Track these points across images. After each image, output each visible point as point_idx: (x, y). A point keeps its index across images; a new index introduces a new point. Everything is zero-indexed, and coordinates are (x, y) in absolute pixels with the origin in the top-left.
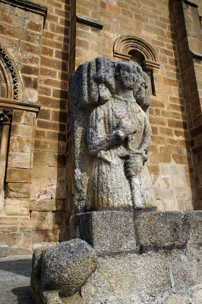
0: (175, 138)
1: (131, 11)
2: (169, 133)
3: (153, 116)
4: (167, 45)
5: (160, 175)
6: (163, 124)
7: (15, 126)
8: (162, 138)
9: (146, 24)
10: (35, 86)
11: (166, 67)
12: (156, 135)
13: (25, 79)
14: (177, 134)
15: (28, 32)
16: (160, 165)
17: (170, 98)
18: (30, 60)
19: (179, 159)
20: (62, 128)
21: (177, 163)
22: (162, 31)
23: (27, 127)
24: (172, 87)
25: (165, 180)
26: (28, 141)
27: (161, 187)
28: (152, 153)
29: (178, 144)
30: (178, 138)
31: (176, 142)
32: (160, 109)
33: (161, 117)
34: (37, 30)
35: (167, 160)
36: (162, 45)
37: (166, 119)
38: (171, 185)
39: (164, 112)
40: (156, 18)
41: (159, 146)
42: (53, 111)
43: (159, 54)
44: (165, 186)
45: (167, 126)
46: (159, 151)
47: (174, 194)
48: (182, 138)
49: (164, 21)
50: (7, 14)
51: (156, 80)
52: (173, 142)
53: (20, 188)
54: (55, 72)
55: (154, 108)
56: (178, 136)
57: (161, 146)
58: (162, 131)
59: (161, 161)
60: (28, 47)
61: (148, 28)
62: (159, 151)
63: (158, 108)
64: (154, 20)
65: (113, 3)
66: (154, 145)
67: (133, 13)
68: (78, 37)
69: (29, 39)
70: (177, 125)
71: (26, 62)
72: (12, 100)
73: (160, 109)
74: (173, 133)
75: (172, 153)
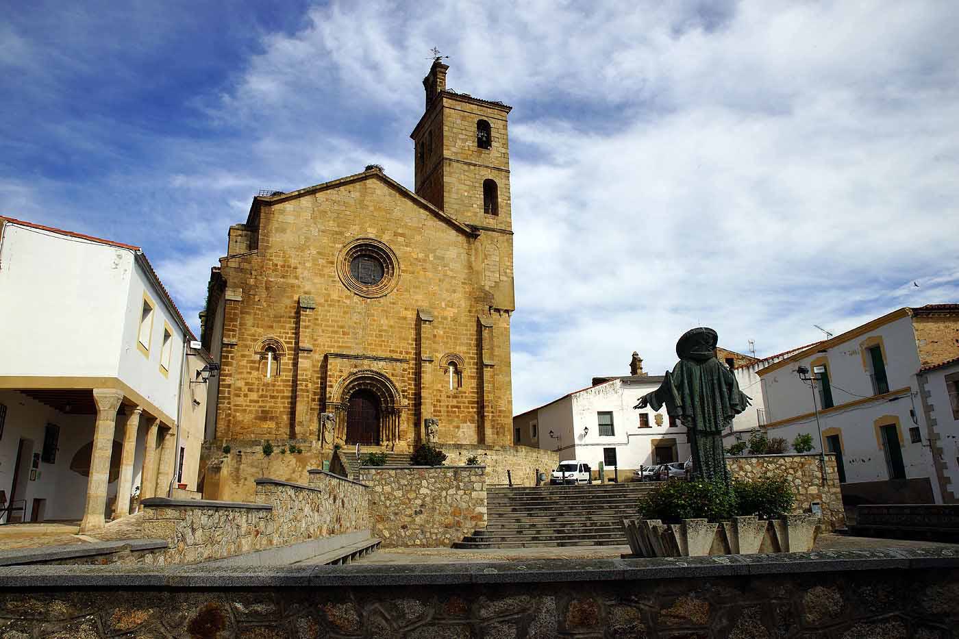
0: (471, 410)
2: (468, 407)
3: (459, 400)
11: (471, 368)
13: (403, 395)
14: (472, 408)
16: (461, 425)
19: (472, 421)
20: (415, 410)
36: (469, 353)
40: (467, 335)
41: (461, 415)
43: (467, 360)
48: (475, 410)
52: (469, 412)
61: (462, 344)
68: (422, 369)
70: (473, 403)
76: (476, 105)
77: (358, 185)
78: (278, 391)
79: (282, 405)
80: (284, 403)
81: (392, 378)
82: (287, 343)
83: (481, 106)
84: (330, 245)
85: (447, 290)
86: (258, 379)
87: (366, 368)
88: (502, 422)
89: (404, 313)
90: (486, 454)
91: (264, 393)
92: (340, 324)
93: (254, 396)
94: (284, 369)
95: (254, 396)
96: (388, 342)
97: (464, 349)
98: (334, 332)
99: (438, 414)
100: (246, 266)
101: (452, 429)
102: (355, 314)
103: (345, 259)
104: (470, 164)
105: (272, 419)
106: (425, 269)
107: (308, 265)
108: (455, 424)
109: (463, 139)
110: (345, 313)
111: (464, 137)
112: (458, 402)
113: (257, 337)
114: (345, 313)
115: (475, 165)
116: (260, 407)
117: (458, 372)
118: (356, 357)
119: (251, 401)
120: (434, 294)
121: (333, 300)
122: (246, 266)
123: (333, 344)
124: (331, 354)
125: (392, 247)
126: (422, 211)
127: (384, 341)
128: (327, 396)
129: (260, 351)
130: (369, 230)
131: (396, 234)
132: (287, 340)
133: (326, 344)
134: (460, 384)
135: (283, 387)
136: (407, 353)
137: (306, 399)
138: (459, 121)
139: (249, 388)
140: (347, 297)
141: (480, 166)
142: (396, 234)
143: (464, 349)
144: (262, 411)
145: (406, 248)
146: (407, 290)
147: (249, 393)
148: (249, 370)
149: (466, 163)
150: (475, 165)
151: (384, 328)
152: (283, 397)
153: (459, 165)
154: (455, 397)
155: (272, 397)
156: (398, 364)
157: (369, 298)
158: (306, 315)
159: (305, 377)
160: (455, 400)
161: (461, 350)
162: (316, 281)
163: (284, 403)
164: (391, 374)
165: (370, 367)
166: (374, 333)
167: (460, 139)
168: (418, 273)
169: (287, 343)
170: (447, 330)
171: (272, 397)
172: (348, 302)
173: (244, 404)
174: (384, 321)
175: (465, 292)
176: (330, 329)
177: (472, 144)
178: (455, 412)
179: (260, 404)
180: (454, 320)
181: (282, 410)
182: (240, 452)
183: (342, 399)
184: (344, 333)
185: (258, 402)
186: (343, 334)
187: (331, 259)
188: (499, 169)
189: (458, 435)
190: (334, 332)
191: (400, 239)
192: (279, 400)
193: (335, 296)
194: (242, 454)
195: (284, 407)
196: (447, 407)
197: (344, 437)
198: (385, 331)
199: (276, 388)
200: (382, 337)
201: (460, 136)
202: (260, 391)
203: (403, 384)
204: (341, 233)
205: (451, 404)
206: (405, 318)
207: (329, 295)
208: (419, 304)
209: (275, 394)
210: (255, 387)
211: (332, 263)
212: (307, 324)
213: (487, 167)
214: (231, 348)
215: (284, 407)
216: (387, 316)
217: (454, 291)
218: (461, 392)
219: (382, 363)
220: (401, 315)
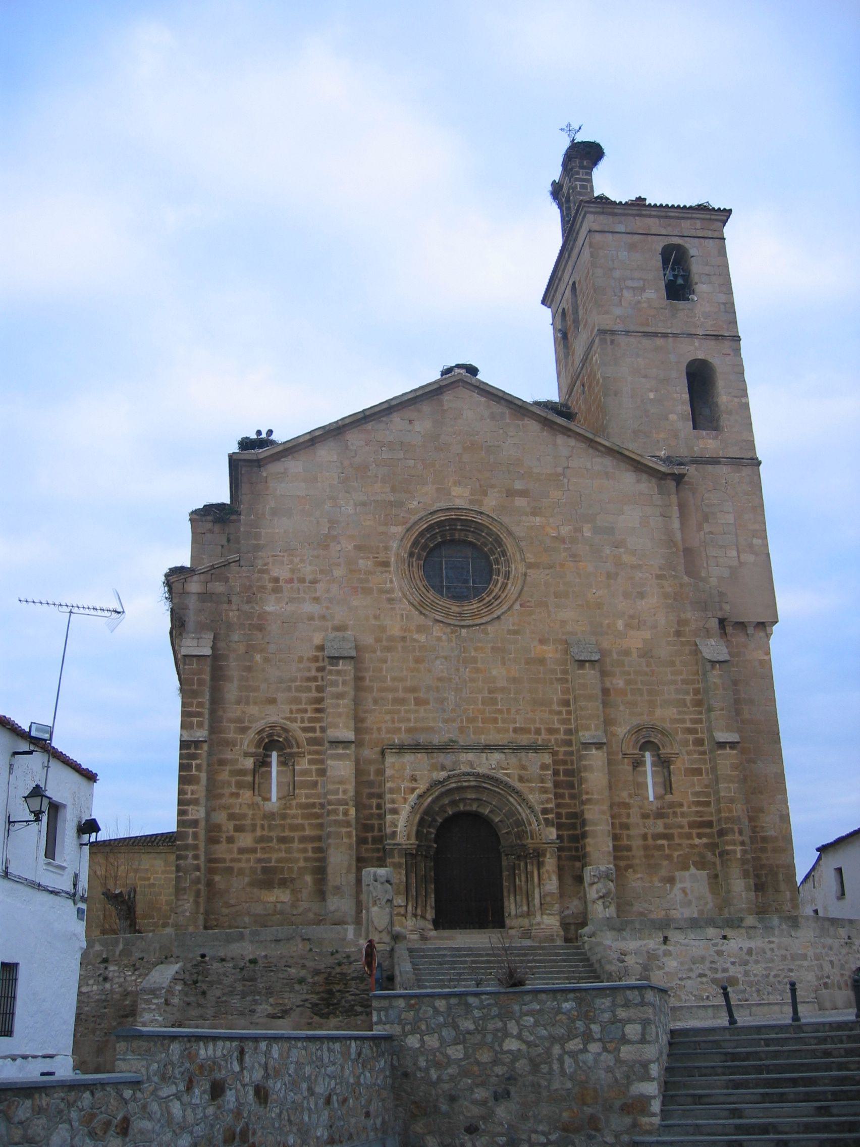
0: (697, 841)
1: (641, 687)
2: (689, 836)
4: (691, 719)
7: (543, 862)
8: (680, 845)
10: (553, 826)
11: (688, 753)
12: (673, 842)
13: (545, 819)
15: (541, 775)
17: (692, 793)
21: (698, 869)
22: (684, 700)
23: (551, 861)
24: (695, 778)
25: (684, 890)
26: (553, 871)
30: (700, 841)
31: (696, 845)
32: (678, 810)
33: (680, 819)
34: (548, 770)
35: (686, 868)
36: (683, 721)
37: (684, 821)
39: (683, 815)
40: (674, 682)
41: (676, 854)
42: (567, 835)
45: (687, 830)
46: (675, 860)
49: (687, 684)
51: (674, 774)
52: (693, 846)
54: (564, 794)
56: (700, 838)
58: (681, 836)
60: (543, 790)
62: (675, 860)
63: (675, 810)
64: (672, 687)
65: (618, 684)
67: (645, 687)
69: (542, 781)
71: (543, 804)
72: (538, 841)
73: (678, 810)
74: (694, 835)
76: (654, 216)
77: (426, 408)
78: (293, 828)
79: (302, 856)
80: (305, 850)
81: (518, 785)
82: (305, 730)
83: (666, 217)
84: (382, 529)
85: (626, 595)
86: (253, 806)
87: (465, 769)
89: (538, 649)
90: (725, 937)
91: (265, 833)
92: (409, 684)
93: (246, 840)
94: (302, 782)
95: (246, 840)
96: (509, 711)
97: (671, 712)
98: (396, 701)
100: (218, 587)
102: (438, 662)
103: (411, 555)
104: (655, 334)
105: (283, 883)
107: (338, 572)
108: (663, 873)
109: (633, 289)
110: (418, 661)
111: (636, 284)
112: (666, 826)
113: (246, 724)
114: (418, 661)
115: (665, 335)
116: (259, 861)
117: (664, 763)
118: (445, 748)
119: (242, 851)
120: (599, 606)
121: (391, 639)
122: (218, 587)
123: (396, 725)
124: (392, 746)
125: (505, 519)
127: (500, 711)
128: (389, 830)
129: (254, 750)
130: (456, 491)
131: (511, 493)
132: (306, 724)
133: (384, 726)
134: (668, 786)
135: (302, 818)
136: (551, 731)
137: (345, 840)
138: (623, 255)
139: (235, 826)
140: (420, 629)
141: (675, 335)
142: (511, 493)
143: (671, 712)
144: (265, 870)
145: (532, 518)
147: (237, 834)
148: (234, 790)
149: (646, 334)
150: (665, 335)
151: (501, 683)
152: (303, 839)
153: (632, 340)
154: (660, 815)
155: (283, 840)
156: (532, 755)
157: (463, 627)
158: (338, 673)
159: (341, 796)
160: (660, 822)
161: (665, 715)
162: (355, 603)
163: (305, 850)
164: (516, 777)
165: (472, 766)
166: (480, 697)
167: (628, 288)
168: (562, 566)
169: (305, 730)
170: (632, 676)
171: (283, 840)
172: (422, 638)
173: (228, 856)
174: (498, 672)
175: (666, 596)
176: (390, 696)
177: (655, 294)
179: (259, 855)
180: (646, 654)
181: (302, 864)
182: (203, 956)
183: (418, 834)
184: (419, 702)
185: (254, 851)
186: (416, 704)
187: (382, 557)
188: (717, 337)
190: (396, 701)
191: (520, 502)
192: (296, 845)
193: (395, 630)
194: (207, 958)
195: (306, 859)
196: (645, 837)
197: (430, 914)
198: (503, 689)
199: (289, 821)
200: (496, 704)
201: (629, 283)
202: (258, 829)
203: (545, 796)
204: (400, 504)
206: (542, 661)
207: (383, 629)
208: (569, 628)
209: (287, 833)
210: (248, 822)
211: (386, 564)
212: (340, 689)
213: (691, 335)
214: (196, 748)
215: (306, 859)
216: (503, 658)
217: (642, 595)
218: (672, 805)
219: (496, 757)
220: (533, 656)
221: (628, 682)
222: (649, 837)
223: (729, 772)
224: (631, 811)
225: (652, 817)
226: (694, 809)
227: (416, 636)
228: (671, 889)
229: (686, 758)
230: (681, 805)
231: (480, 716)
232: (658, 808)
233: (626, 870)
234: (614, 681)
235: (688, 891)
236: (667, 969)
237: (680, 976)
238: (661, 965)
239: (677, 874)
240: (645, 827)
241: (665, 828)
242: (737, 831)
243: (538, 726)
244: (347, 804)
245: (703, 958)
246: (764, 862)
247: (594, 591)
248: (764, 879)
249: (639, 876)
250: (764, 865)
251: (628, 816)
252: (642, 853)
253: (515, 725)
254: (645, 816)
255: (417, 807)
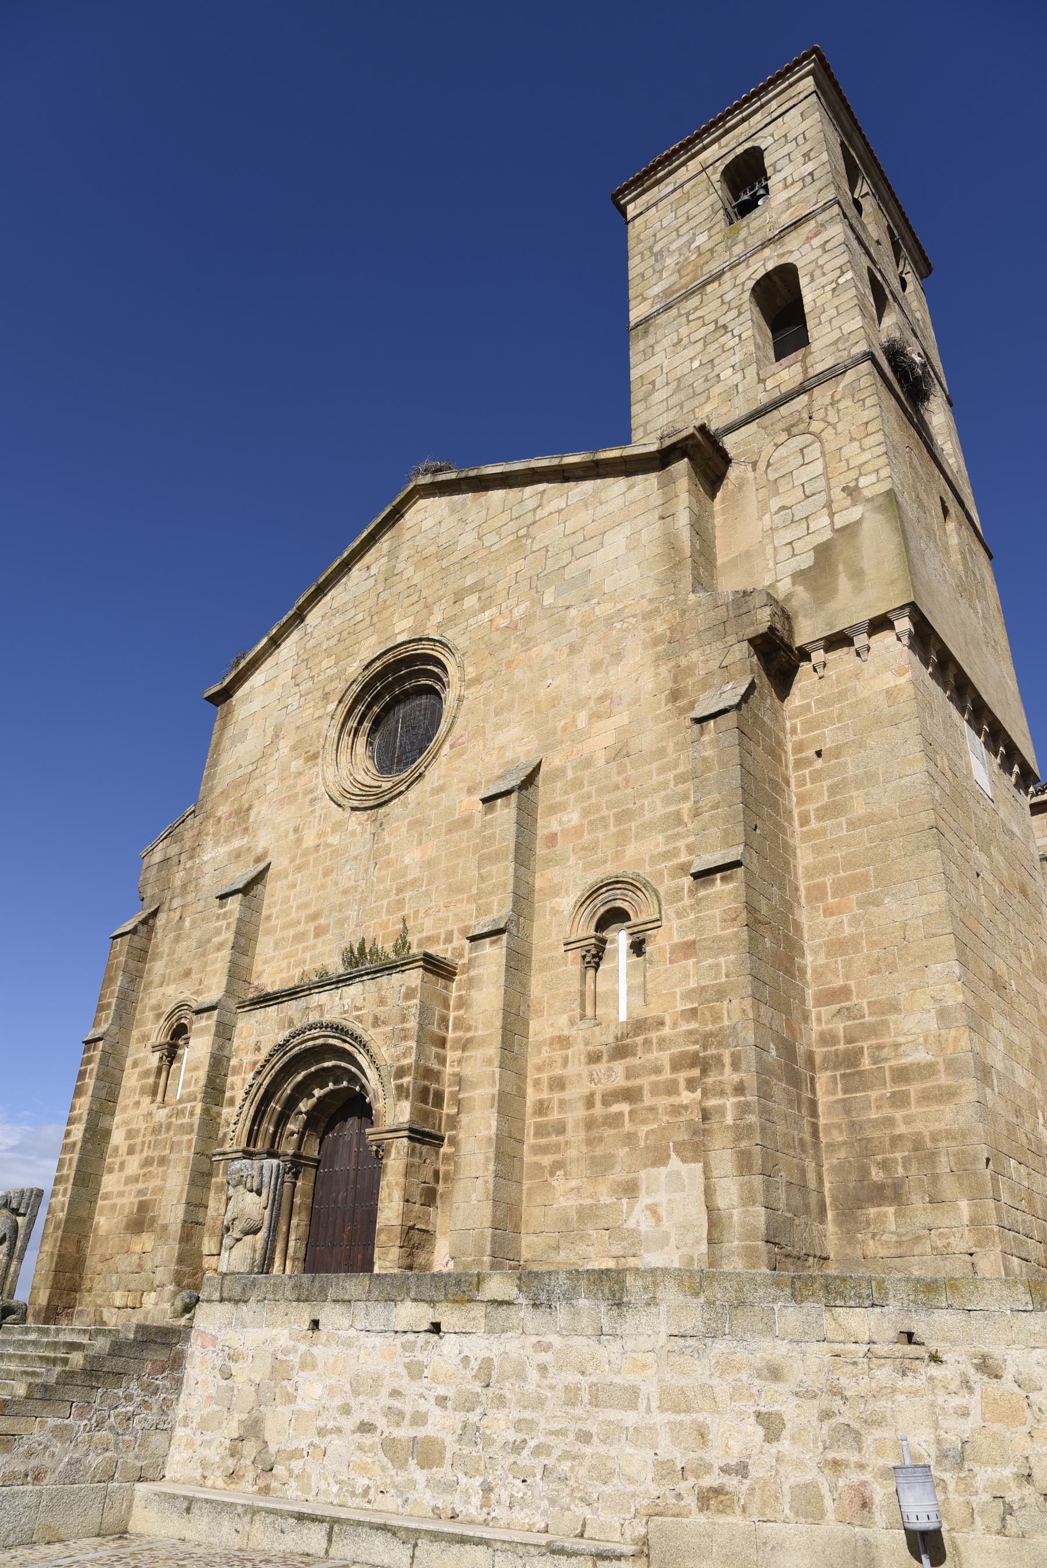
2: (671, 1088)
5: (641, 1199)
6: (658, 1070)
8: (652, 1109)
9: (640, 821)
12: (639, 1105)
18: (404, 1054)
21: (684, 1160)
25: (653, 1210)
26: (397, 1184)
27: (643, 1228)
28: (627, 1149)
29: (691, 1113)
31: (686, 1107)
32: (653, 1035)
33: (656, 1054)
35: (659, 1158)
38: (665, 1220)
44: (652, 1222)
45: (667, 1075)
46: (642, 1143)
47: (673, 1242)
49: (685, 781)
50: (383, 993)
52: (676, 1110)
53: (387, 1254)
55: (639, 1040)
57: (647, 1128)
59: (645, 1166)
60: (402, 1035)
62: (642, 1143)
64: (657, 798)
66: (632, 1129)
74: (682, 1085)
75: (675, 1139)
88: (918, 1126)
90: (436, 1328)
99: (554, 1139)
101: (605, 1199)
106: (528, 644)
108: (619, 1174)
110: (327, 873)
112: (630, 1073)
126: (529, 490)
140: (338, 827)
146: (479, 732)
178: (615, 1120)
180: (619, 753)
189: (631, 1224)
198: (414, 883)
205: (599, 1089)
208: (509, 755)
217: (618, 656)
221: (586, 812)
222: (598, 1099)
223: (719, 933)
224: (569, 1052)
225: (605, 1058)
226: (685, 1027)
227: (330, 840)
228: (631, 1208)
229: (675, 924)
230: (661, 1023)
231: (381, 933)
232: (617, 1038)
233: (552, 1174)
234: (565, 819)
235: (662, 1212)
236: (300, 1405)
237: (320, 1423)
238: (291, 1390)
239: (643, 1174)
240: (592, 1080)
241: (627, 1078)
242: (727, 1060)
243: (450, 928)
244: (195, 1099)
245: (377, 1380)
246: (902, 1129)
247: (549, 681)
248: (900, 1171)
249: (573, 1183)
250: (900, 1137)
251: (565, 1061)
252: (582, 1134)
253: (420, 936)
254: (594, 1058)
255: (254, 1090)
